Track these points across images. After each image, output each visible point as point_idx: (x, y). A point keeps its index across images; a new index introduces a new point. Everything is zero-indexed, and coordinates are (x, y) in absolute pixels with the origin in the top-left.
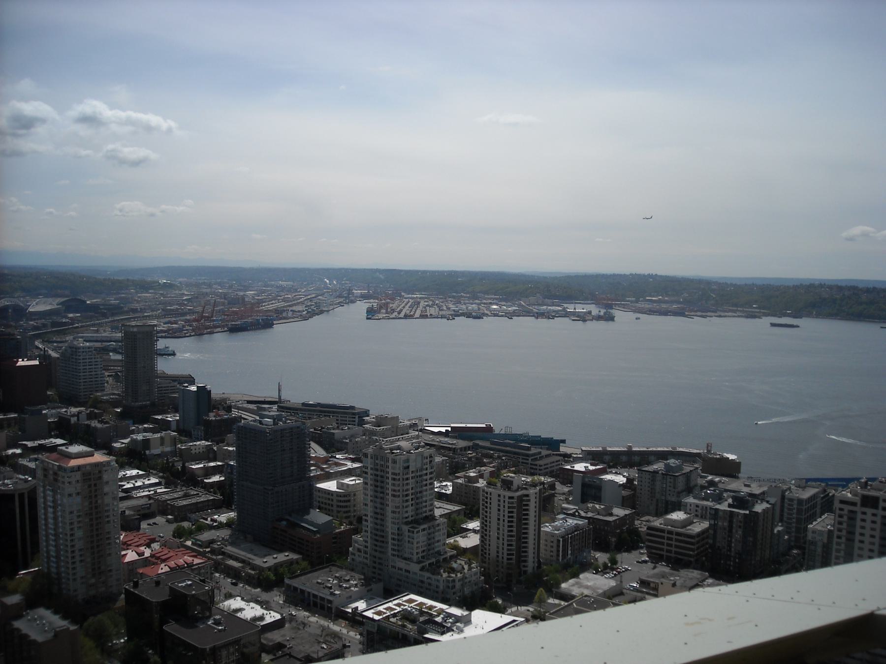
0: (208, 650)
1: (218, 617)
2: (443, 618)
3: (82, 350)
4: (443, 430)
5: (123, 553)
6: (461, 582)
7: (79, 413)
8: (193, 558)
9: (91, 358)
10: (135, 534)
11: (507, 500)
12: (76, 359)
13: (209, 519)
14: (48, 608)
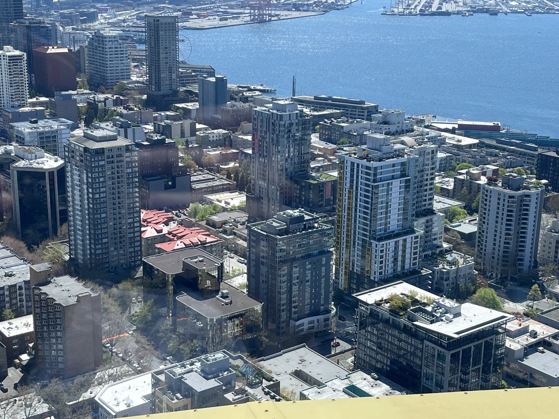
0: (215, 320)
1: (225, 291)
2: (433, 308)
3: (108, 40)
4: (450, 127)
5: (143, 229)
6: (455, 275)
7: (106, 99)
8: (205, 237)
9: (117, 48)
10: (154, 213)
11: (507, 199)
12: (103, 48)
13: (223, 202)
14: (72, 276)
